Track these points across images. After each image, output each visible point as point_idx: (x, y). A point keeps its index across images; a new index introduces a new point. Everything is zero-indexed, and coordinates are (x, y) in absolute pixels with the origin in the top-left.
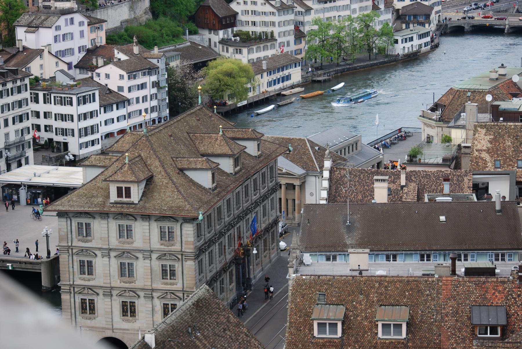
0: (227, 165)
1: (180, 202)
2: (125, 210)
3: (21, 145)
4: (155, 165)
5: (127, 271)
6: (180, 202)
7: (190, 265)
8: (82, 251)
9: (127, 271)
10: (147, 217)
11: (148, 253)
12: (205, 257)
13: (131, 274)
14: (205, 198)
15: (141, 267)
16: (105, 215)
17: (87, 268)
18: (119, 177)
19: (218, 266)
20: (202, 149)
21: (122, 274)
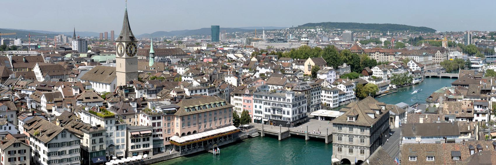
0: (378, 113)
1: (366, 122)
2: (351, 123)
3: (318, 105)
4: (359, 112)
5: (351, 140)
6: (366, 122)
7: (368, 139)
8: (339, 134)
9: (351, 140)
10: (357, 126)
11: (357, 136)
12: (372, 137)
13: (352, 141)
14: (373, 121)
15: (355, 139)
16: (345, 125)
17: (340, 139)
18: (350, 115)
19: (375, 140)
20: (371, 108)
21: (350, 141)
